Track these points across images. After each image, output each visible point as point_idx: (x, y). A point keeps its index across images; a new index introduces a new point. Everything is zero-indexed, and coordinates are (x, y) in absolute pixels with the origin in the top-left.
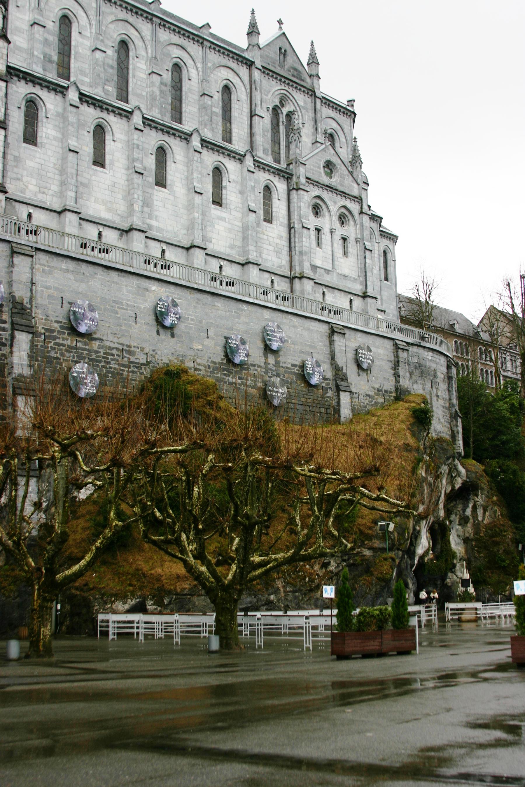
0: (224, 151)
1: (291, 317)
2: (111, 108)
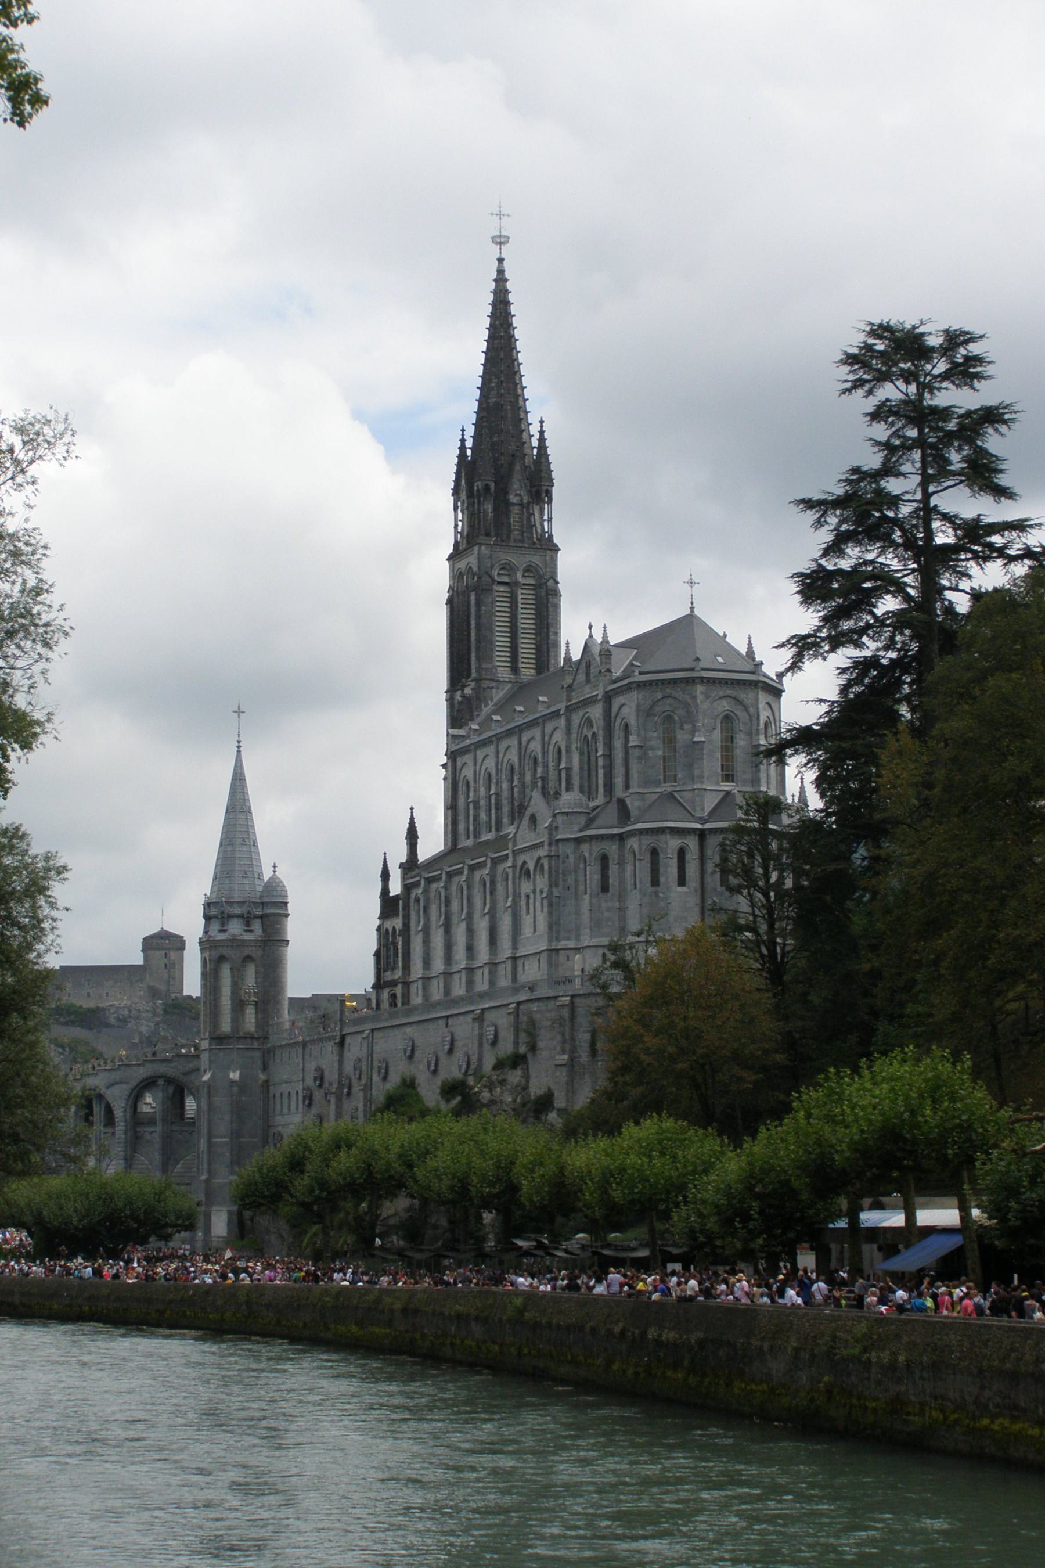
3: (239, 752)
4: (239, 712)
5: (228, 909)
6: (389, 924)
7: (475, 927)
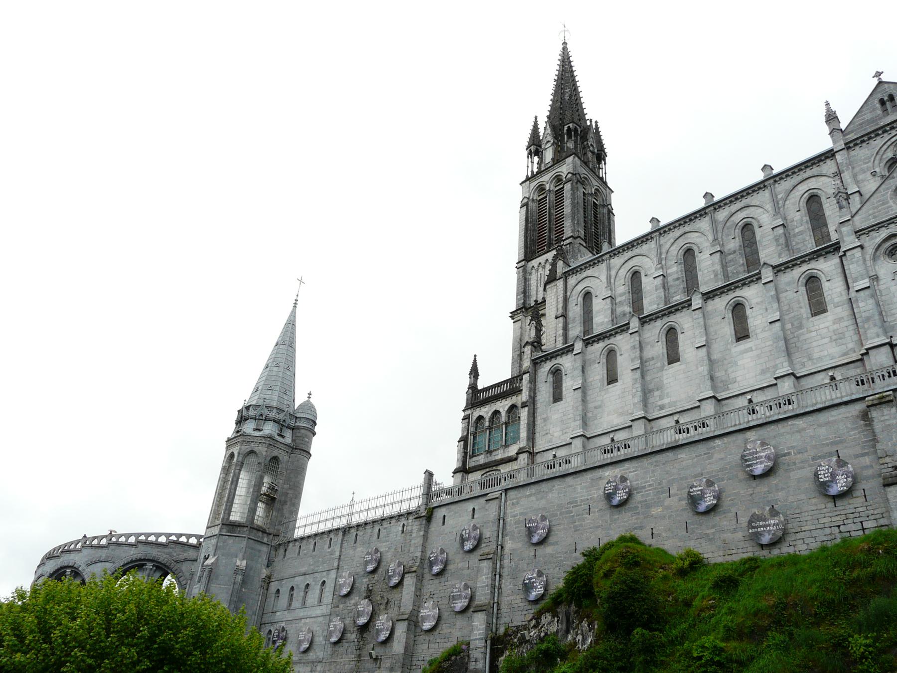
0: (736, 285)
1: (790, 422)
2: (613, 332)
3: (295, 307)
4: (301, 281)
5: (266, 412)
6: (486, 411)
7: (715, 356)
